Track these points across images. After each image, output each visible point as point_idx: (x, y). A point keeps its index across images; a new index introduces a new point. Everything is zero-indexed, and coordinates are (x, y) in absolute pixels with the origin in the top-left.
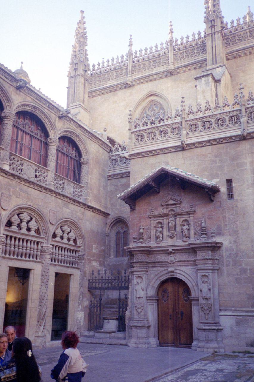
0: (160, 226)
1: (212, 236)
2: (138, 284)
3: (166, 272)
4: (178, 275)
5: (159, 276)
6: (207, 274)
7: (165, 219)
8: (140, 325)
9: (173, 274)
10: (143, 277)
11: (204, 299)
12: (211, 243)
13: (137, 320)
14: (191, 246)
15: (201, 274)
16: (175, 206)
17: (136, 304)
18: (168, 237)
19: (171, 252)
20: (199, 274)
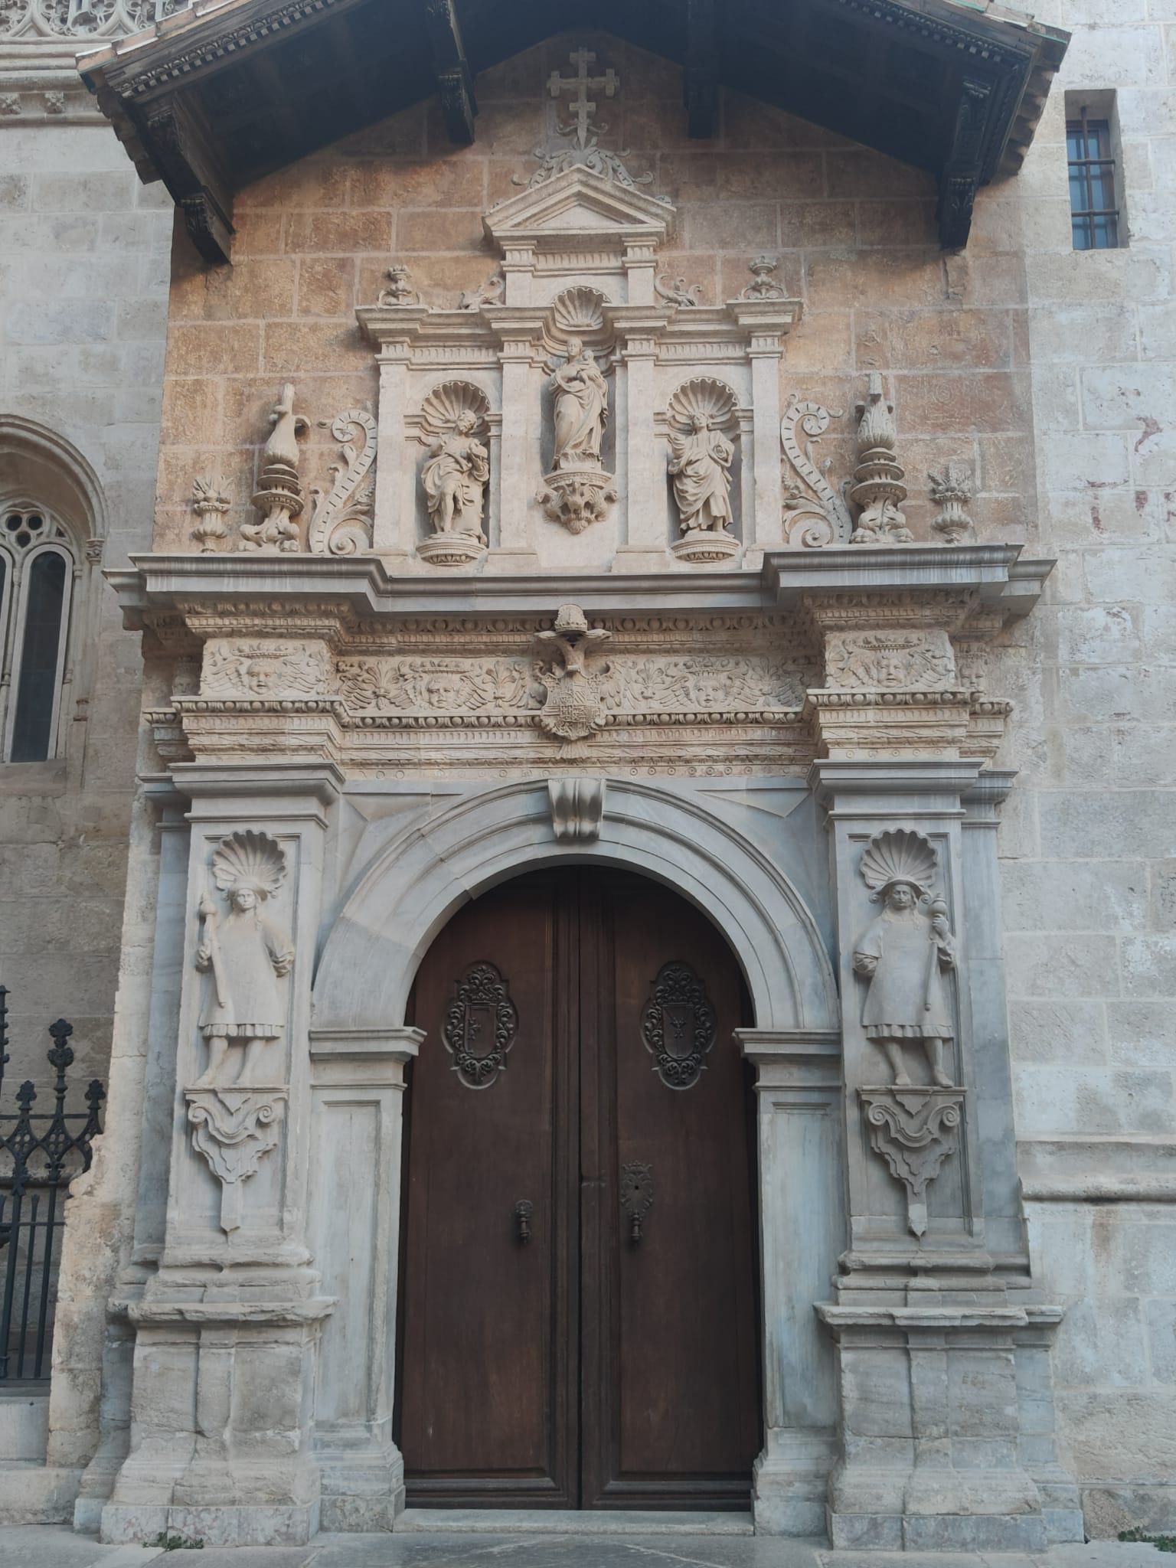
0: (469, 417)
1: (942, 528)
2: (244, 911)
3: (525, 805)
4: (631, 835)
5: (440, 844)
6: (923, 829)
7: (519, 360)
8: (236, 1311)
9: (587, 827)
10: (282, 846)
11: (895, 1051)
12: (978, 556)
13: (199, 1265)
14: (787, 581)
15: (858, 828)
16: (614, 262)
17: (205, 1101)
18: (538, 515)
19: (574, 637)
20: (842, 830)
